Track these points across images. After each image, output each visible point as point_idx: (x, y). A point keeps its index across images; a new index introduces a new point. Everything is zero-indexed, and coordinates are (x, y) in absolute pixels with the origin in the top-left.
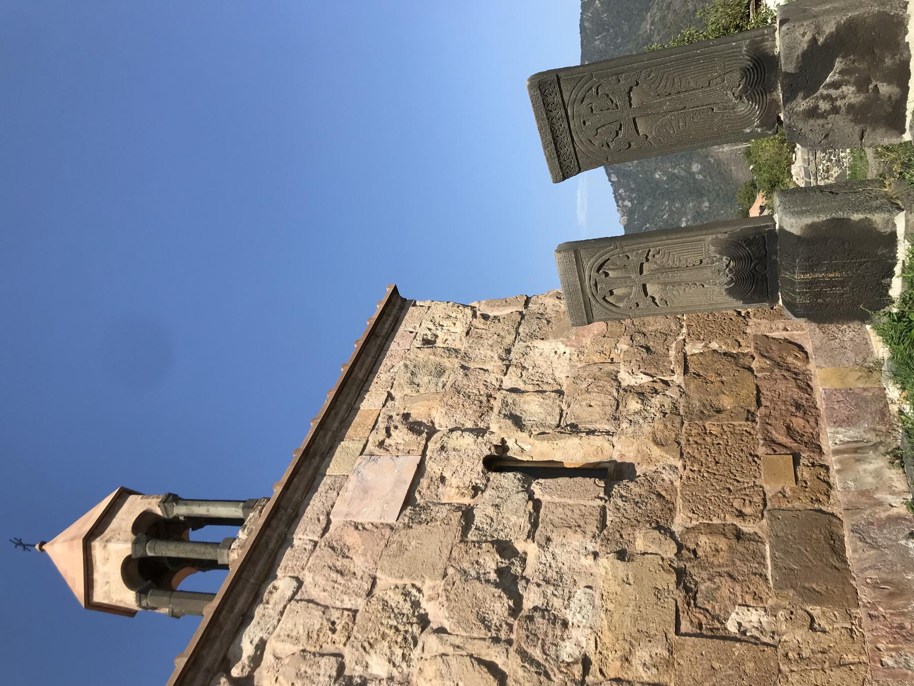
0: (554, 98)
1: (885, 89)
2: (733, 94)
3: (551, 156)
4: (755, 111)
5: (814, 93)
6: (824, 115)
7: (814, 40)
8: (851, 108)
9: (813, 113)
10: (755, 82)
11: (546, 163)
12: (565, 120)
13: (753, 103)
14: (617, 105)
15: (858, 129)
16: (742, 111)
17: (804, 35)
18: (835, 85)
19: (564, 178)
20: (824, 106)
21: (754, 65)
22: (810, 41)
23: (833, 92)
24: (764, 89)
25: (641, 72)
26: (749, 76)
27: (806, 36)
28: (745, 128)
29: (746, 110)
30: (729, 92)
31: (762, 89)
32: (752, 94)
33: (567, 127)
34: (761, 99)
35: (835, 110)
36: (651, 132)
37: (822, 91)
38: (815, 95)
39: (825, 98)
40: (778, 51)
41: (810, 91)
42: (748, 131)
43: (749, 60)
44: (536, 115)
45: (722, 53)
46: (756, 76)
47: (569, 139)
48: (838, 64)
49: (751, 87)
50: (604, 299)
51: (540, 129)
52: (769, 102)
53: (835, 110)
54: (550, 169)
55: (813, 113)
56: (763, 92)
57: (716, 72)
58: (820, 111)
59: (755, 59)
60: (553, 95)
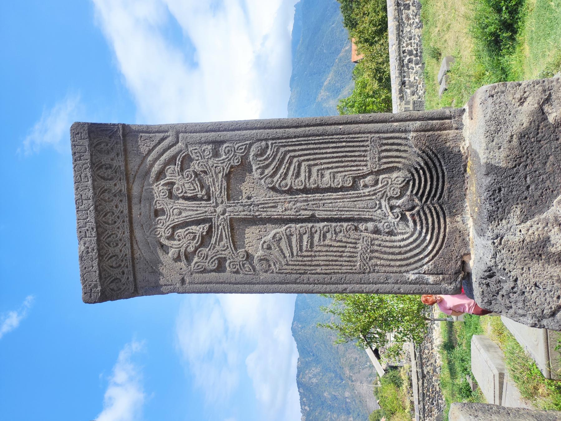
0: (112, 160)
2: (392, 208)
3: (88, 252)
4: (425, 244)
5: (541, 212)
10: (426, 193)
11: (79, 263)
12: (125, 199)
13: (422, 228)
14: (208, 194)
16: (403, 240)
17: (522, 101)
19: (104, 298)
21: (426, 163)
22: (532, 114)
24: (442, 209)
25: (251, 145)
26: (417, 182)
27: (525, 104)
28: (407, 272)
29: (411, 240)
30: (384, 203)
31: (438, 208)
32: (422, 213)
33: (126, 212)
34: (436, 225)
36: (256, 251)
38: (543, 216)
40: (467, 145)
42: (412, 277)
43: (419, 155)
44: (76, 176)
45: (377, 135)
46: (429, 183)
47: (127, 234)
49: (421, 200)
51: (79, 201)
52: (449, 232)
54: (82, 276)
56: (441, 213)
57: (366, 165)
58: (553, 250)
59: (427, 155)
60: (112, 155)
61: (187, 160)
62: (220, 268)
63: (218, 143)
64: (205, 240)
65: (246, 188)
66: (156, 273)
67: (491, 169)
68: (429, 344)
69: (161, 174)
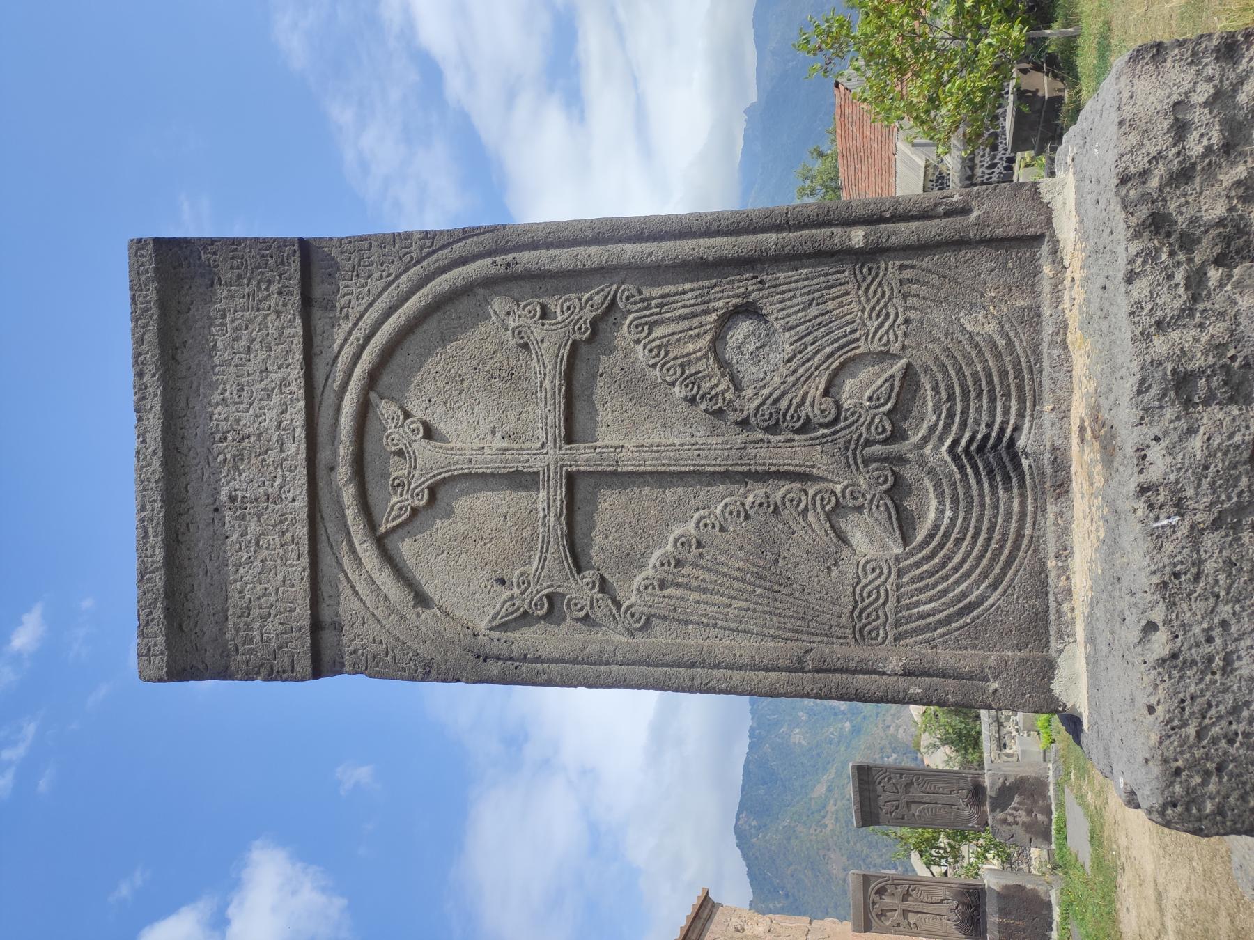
1: (1041, 817)
6: (1010, 824)
7: (1004, 783)
8: (1024, 823)
9: (1004, 821)
15: (1028, 836)
18: (1016, 809)
20: (1010, 819)
23: (1014, 812)
35: (1016, 823)
37: (1009, 810)
39: (1011, 815)
41: (1003, 809)
48: (1017, 798)
50: (877, 915)
53: (1016, 823)
55: (1004, 821)
61: (890, 779)
62: (903, 818)
63: (902, 774)
64: (897, 807)
65: (911, 790)
66: (878, 818)
67: (991, 797)
68: (1025, 865)
69: (880, 783)
